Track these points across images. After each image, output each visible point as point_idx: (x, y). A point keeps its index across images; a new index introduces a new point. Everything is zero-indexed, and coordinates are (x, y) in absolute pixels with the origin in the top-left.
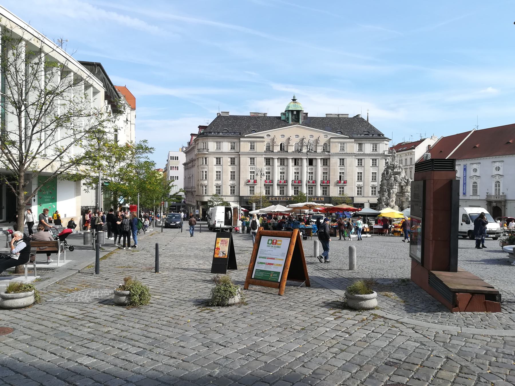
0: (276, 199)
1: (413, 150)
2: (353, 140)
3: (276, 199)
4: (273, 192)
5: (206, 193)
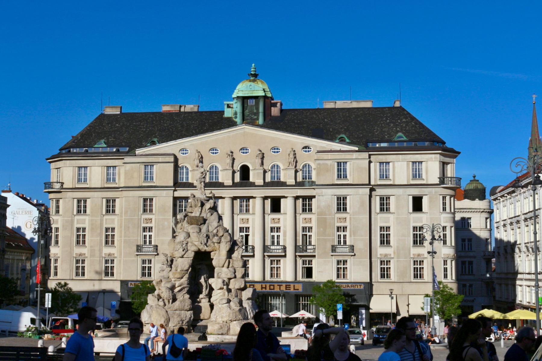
2: (366, 155)
5: (56, 274)
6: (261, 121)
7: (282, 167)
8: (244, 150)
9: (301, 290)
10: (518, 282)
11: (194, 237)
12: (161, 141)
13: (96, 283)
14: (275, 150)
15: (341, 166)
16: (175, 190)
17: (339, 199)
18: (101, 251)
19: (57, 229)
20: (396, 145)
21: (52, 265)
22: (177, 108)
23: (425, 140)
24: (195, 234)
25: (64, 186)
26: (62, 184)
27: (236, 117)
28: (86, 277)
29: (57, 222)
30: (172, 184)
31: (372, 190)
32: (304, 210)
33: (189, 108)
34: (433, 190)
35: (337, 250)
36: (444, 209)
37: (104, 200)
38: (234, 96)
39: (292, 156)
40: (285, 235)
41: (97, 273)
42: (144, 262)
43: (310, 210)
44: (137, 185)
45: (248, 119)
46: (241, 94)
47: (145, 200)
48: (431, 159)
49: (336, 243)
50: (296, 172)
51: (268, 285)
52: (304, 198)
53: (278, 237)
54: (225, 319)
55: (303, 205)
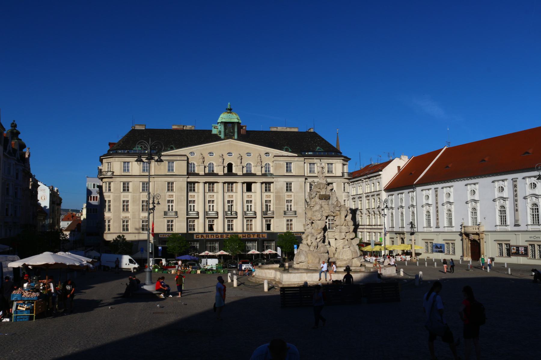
0: (202, 236)
1: (380, 173)
2: (302, 159)
3: (202, 236)
4: (198, 228)
5: (109, 230)
6: (236, 137)
7: (253, 165)
8: (230, 154)
9: (266, 237)
10: (358, 230)
11: (326, 207)
12: (178, 148)
13: (136, 235)
14: (249, 154)
15: (288, 164)
16: (188, 178)
17: (287, 184)
18: (139, 215)
19: (109, 201)
20: (317, 153)
21: (107, 224)
22: (182, 127)
23: (332, 152)
24: (326, 205)
25: (114, 174)
26: (113, 172)
27: (220, 134)
28: (130, 231)
29: (109, 197)
30: (186, 174)
31: (306, 179)
32: (266, 190)
33: (188, 127)
34: (339, 180)
35: (287, 214)
36: (344, 190)
37: (141, 183)
38: (219, 121)
39: (259, 158)
40: (217, 205)
41: (136, 229)
42: (168, 221)
43: (270, 190)
44: (164, 174)
45: (228, 136)
46: (224, 120)
47: (168, 183)
48: (337, 162)
49: (286, 210)
50: (262, 167)
51: (246, 235)
52: (266, 183)
53: (251, 206)
54: (349, 257)
55: (209, 187)
